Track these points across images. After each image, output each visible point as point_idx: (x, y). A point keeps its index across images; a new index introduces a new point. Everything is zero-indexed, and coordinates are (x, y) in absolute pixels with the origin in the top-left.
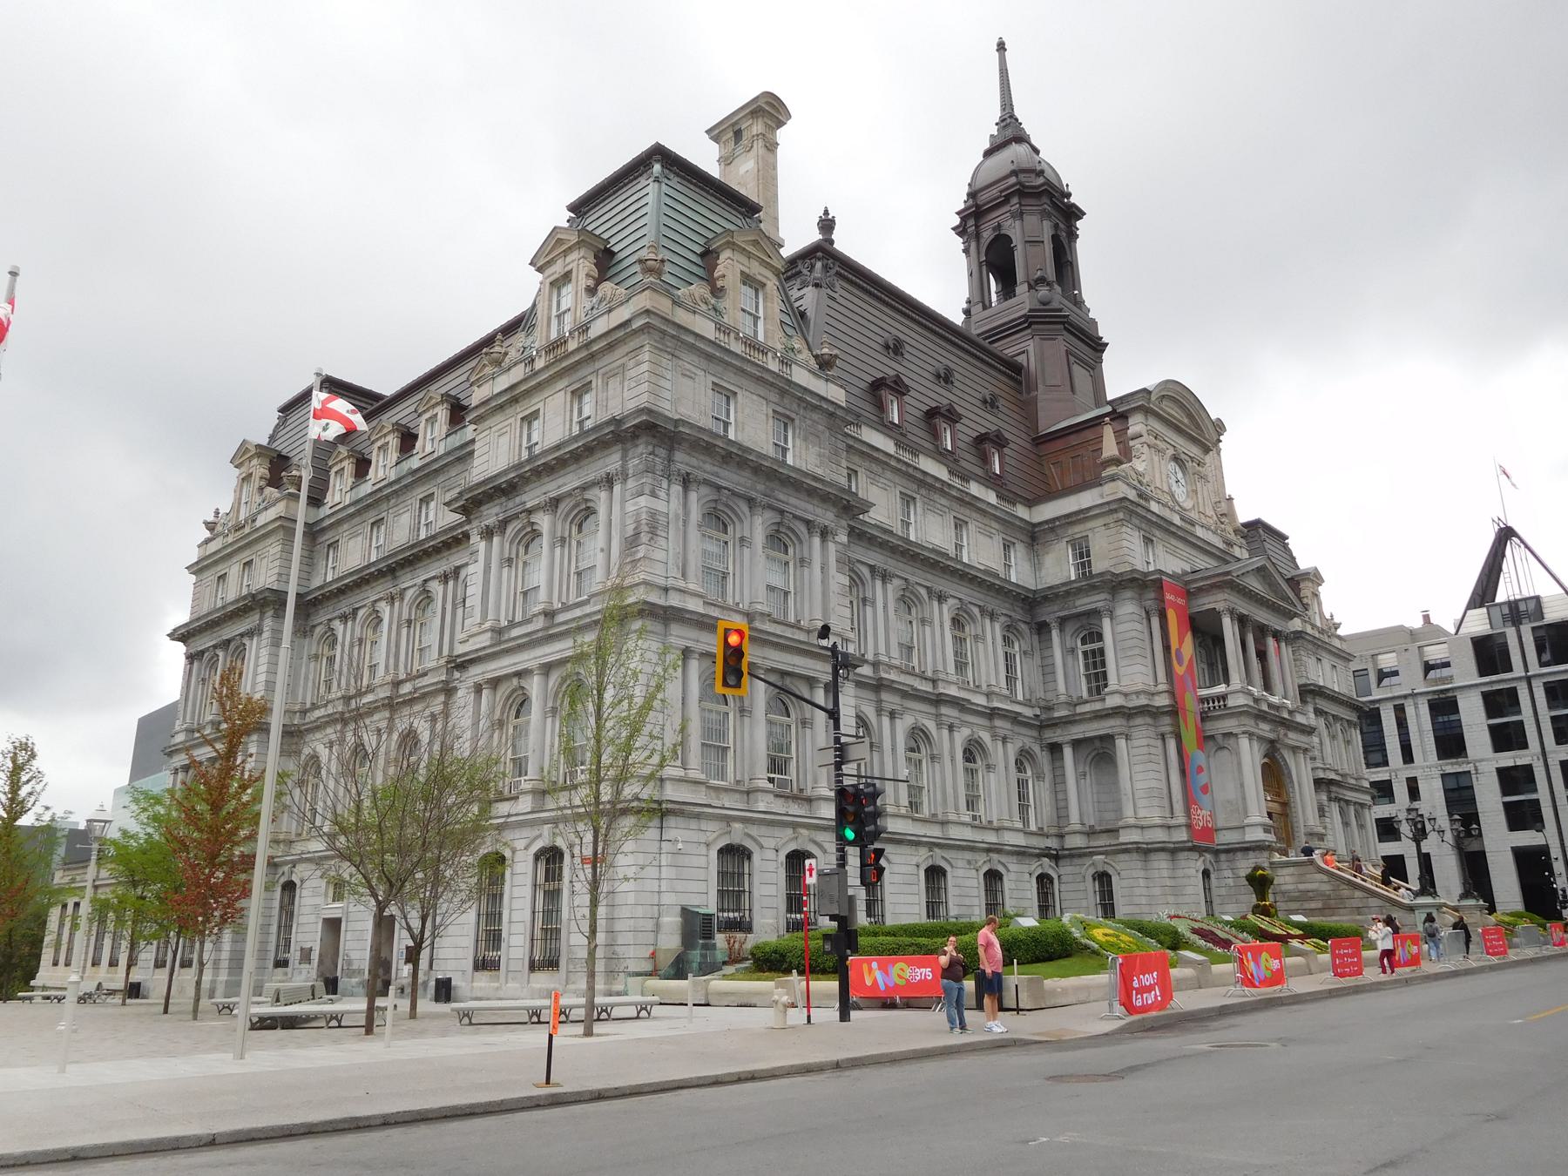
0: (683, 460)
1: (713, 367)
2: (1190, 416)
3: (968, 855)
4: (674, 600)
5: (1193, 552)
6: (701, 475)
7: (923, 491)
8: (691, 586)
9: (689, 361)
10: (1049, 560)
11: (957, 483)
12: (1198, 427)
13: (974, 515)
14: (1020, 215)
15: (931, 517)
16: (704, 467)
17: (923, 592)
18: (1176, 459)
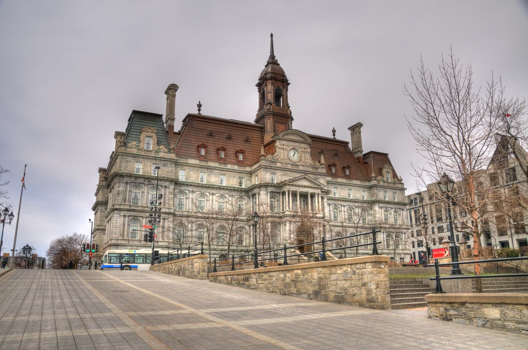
0: (125, 179)
1: (136, 158)
2: (301, 136)
4: (122, 207)
5: (296, 173)
6: (130, 181)
7: (209, 170)
8: (127, 203)
9: (129, 159)
10: (253, 180)
11: (222, 166)
13: (228, 173)
14: (266, 85)
15: (211, 175)
16: (133, 180)
17: (207, 194)
18: (294, 149)
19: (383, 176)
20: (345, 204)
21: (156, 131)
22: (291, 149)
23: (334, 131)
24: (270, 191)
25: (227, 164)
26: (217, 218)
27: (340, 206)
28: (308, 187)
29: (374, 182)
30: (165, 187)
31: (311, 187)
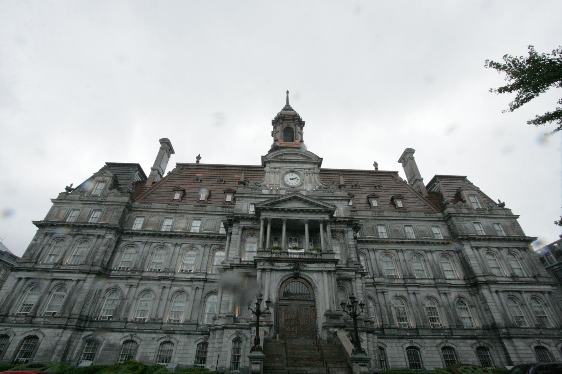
3: (154, 335)
7: (178, 215)
12: (309, 158)
13: (205, 216)
18: (292, 172)
19: (465, 201)
20: (404, 247)
21: (111, 174)
22: (287, 173)
23: (376, 165)
24: (242, 226)
25: (205, 206)
26: (173, 279)
27: (394, 252)
28: (302, 211)
29: (450, 210)
30: (99, 236)
31: (308, 211)
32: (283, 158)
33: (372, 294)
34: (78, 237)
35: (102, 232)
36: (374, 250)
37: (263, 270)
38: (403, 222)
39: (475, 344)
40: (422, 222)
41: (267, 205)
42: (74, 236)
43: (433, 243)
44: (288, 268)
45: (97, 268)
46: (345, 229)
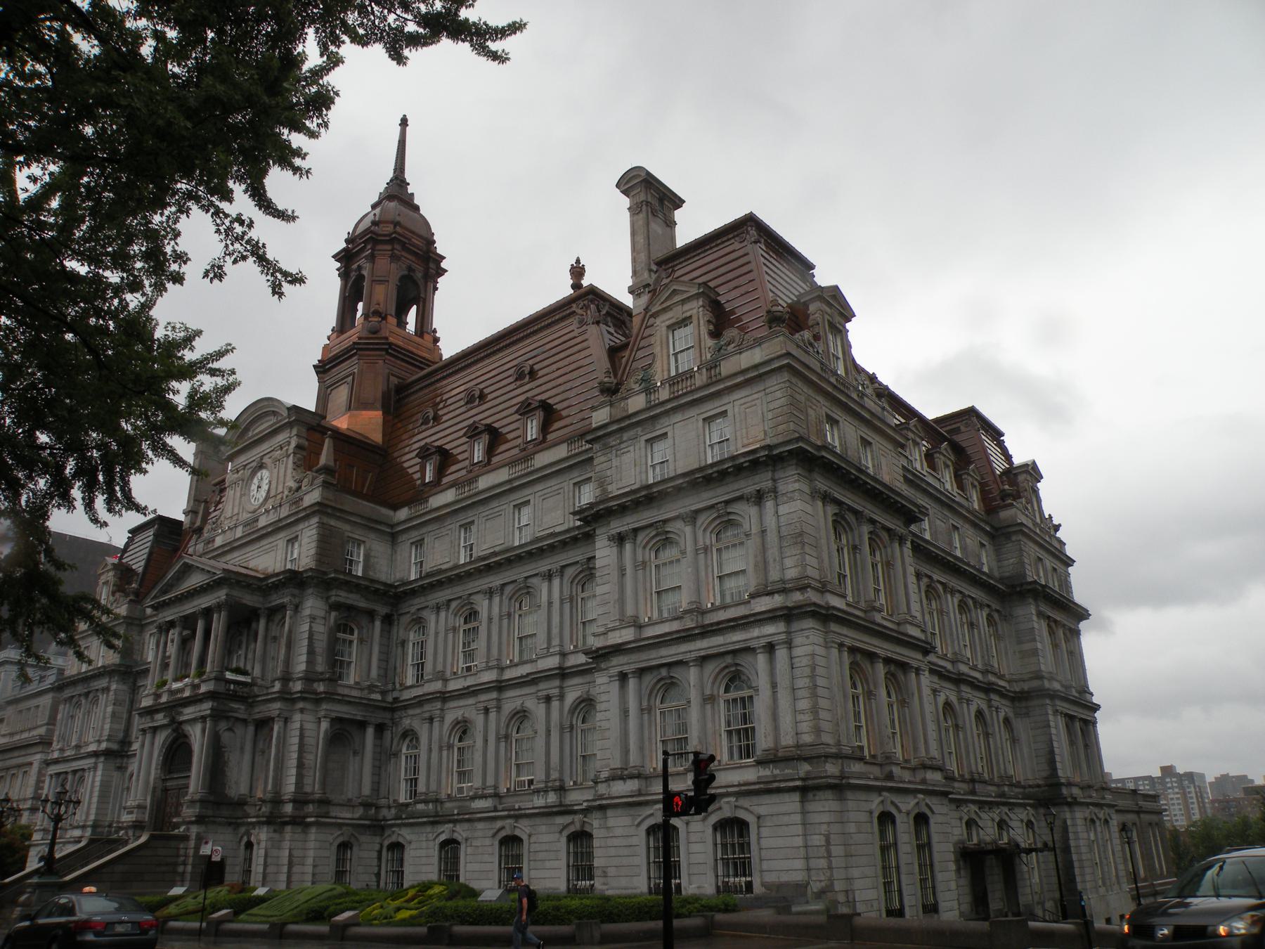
18: (261, 466)
20: (495, 581)
22: (254, 473)
30: (103, 689)
32: (250, 434)
33: (415, 724)
34: (91, 696)
35: (103, 683)
36: (438, 608)
37: (144, 731)
38: (513, 496)
39: (565, 827)
40: (553, 482)
41: (155, 597)
42: (87, 695)
43: (552, 548)
44: (165, 722)
45: (104, 746)
46: (286, 600)
